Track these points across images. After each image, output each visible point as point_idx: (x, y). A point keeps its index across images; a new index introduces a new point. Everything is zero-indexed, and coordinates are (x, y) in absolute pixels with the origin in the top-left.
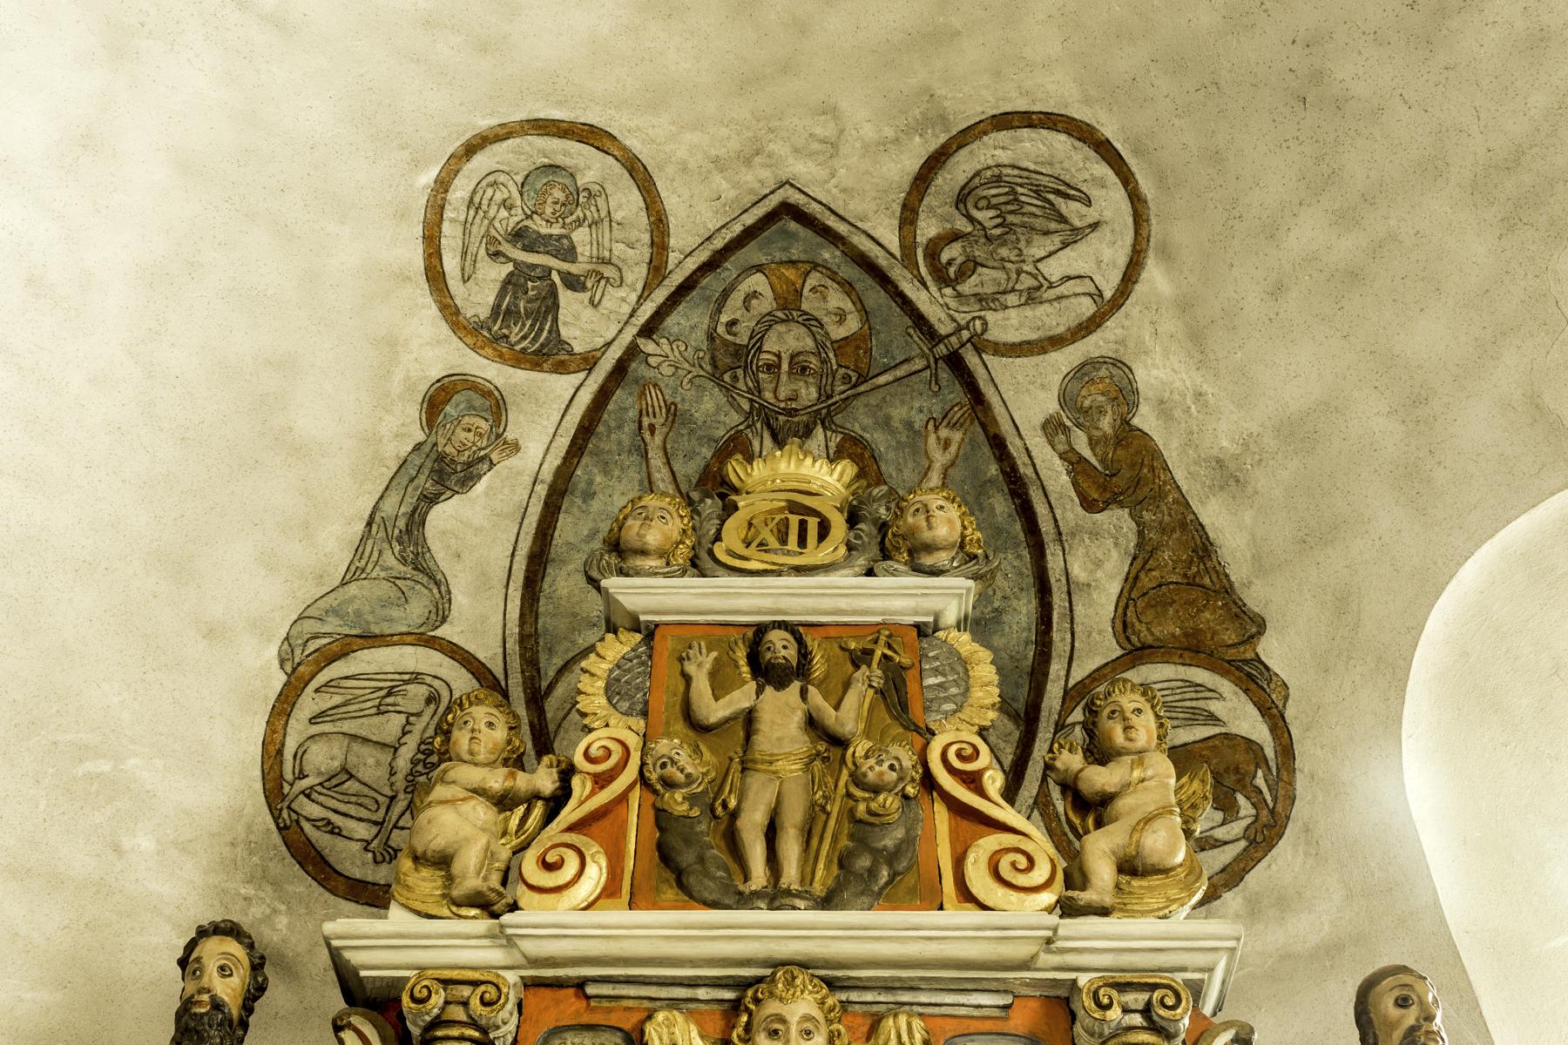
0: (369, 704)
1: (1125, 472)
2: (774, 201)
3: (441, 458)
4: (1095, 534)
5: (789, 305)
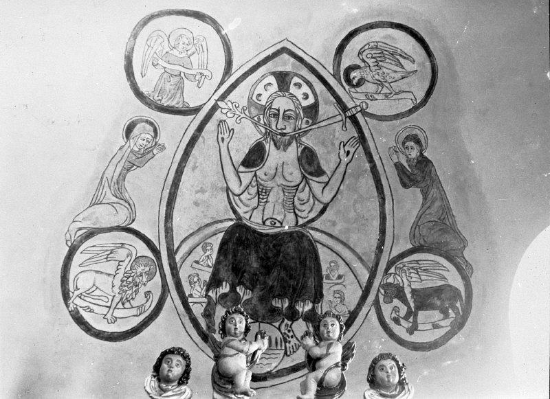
0: (103, 257)
1: (418, 173)
2: (279, 47)
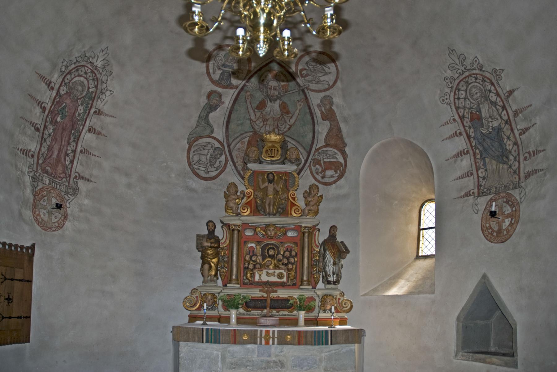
1: (329, 116)
3: (211, 105)
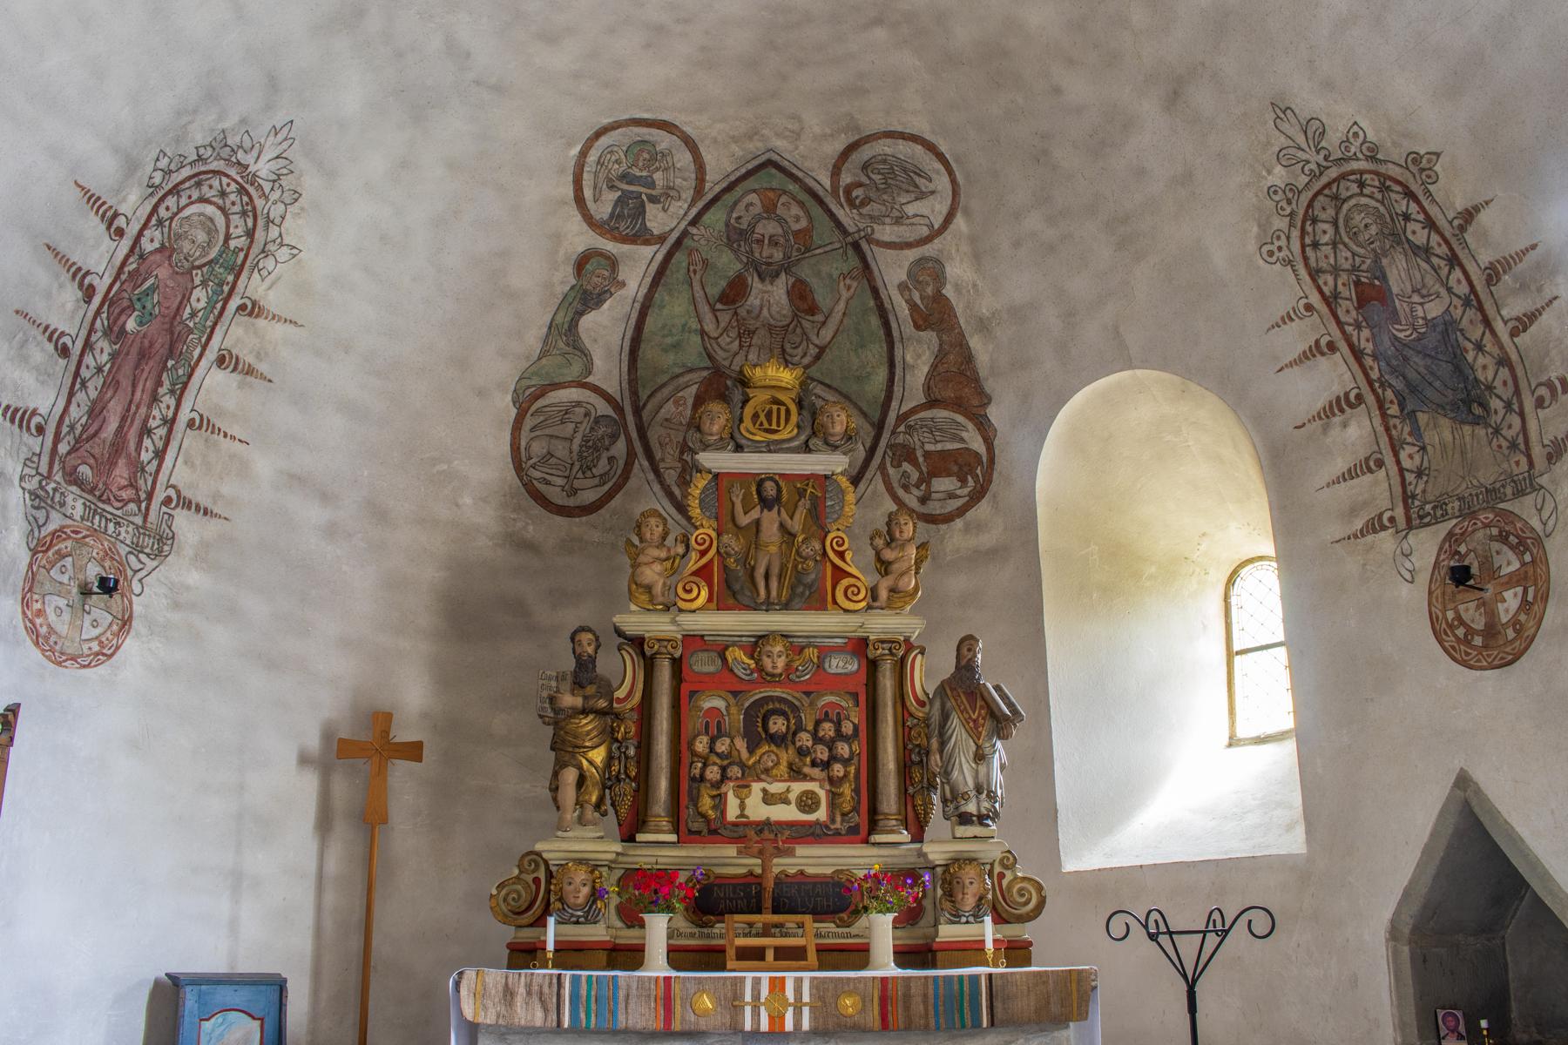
1: (935, 314)
3: (585, 292)
4: (919, 341)
5: (770, 209)
